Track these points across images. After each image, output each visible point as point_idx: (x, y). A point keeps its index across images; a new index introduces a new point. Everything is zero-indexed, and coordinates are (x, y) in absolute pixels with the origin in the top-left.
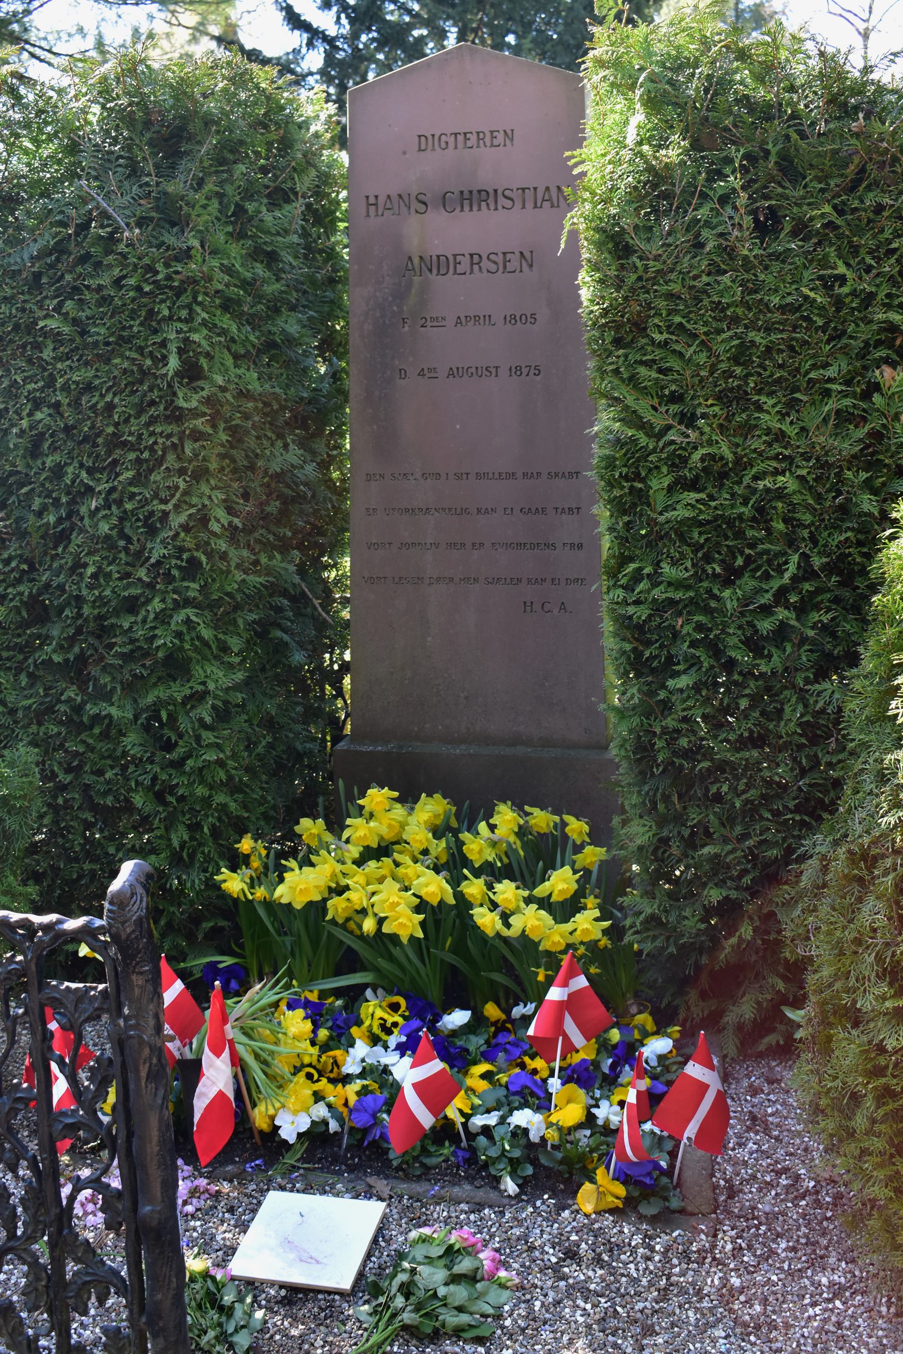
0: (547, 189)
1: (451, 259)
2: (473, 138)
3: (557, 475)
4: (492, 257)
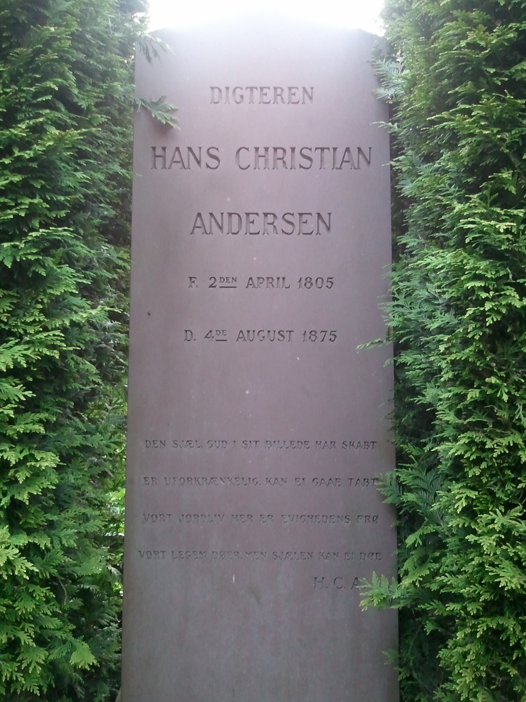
0: (348, 150)
1: (244, 217)
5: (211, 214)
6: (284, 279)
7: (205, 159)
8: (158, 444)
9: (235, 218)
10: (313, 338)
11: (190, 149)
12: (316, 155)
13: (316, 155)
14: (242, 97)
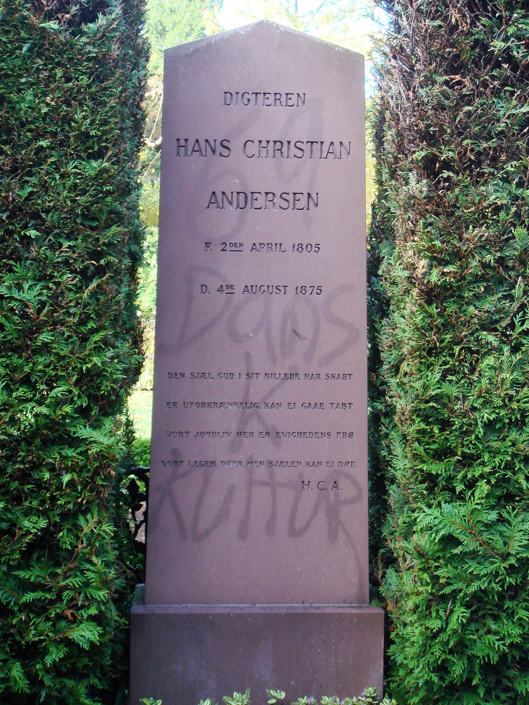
0: (332, 143)
1: (249, 195)
2: (272, 97)
3: (333, 376)
4: (284, 196)
5: (223, 193)
6: (281, 244)
7: (219, 149)
8: (179, 375)
9: (242, 196)
10: (303, 292)
11: (207, 141)
12: (306, 147)
13: (306, 147)
14: (249, 100)
